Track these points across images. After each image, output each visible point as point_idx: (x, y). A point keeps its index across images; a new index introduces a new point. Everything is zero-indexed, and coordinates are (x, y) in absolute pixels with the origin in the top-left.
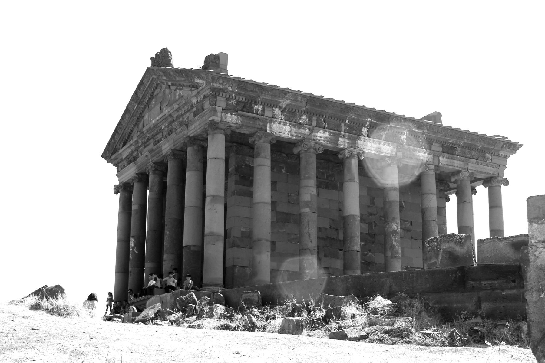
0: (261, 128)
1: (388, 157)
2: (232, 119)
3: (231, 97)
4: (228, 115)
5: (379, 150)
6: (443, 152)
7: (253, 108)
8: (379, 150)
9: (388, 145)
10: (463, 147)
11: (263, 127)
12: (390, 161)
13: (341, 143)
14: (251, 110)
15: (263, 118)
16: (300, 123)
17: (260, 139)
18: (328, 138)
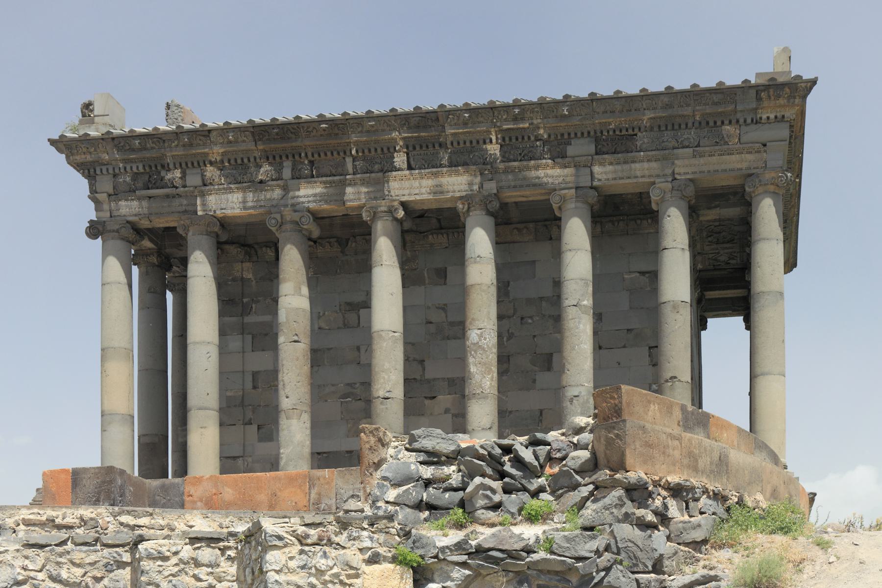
0: (185, 211)
1: (461, 198)
2: (129, 208)
3: (117, 171)
4: (123, 203)
5: (438, 190)
6: (597, 154)
7: (162, 179)
8: (438, 190)
9: (458, 174)
10: (652, 129)
11: (190, 208)
12: (466, 206)
13: (352, 197)
14: (160, 183)
15: (186, 192)
16: (261, 182)
17: (186, 229)
18: (321, 195)
